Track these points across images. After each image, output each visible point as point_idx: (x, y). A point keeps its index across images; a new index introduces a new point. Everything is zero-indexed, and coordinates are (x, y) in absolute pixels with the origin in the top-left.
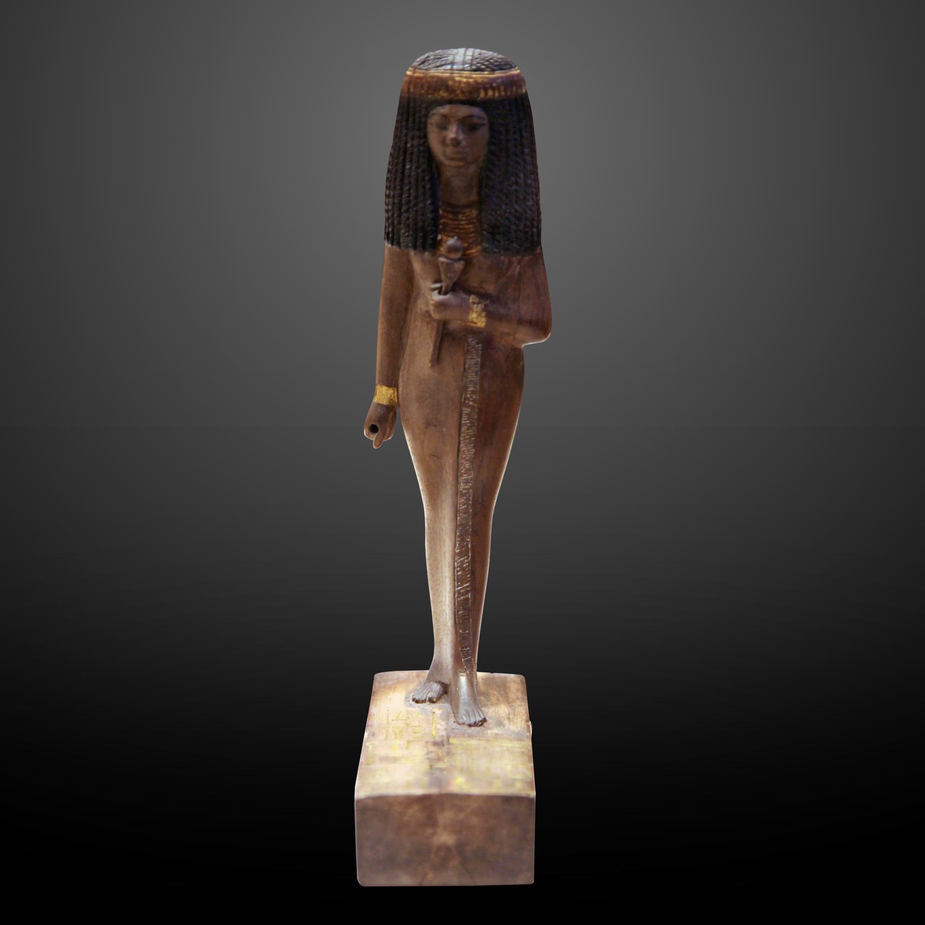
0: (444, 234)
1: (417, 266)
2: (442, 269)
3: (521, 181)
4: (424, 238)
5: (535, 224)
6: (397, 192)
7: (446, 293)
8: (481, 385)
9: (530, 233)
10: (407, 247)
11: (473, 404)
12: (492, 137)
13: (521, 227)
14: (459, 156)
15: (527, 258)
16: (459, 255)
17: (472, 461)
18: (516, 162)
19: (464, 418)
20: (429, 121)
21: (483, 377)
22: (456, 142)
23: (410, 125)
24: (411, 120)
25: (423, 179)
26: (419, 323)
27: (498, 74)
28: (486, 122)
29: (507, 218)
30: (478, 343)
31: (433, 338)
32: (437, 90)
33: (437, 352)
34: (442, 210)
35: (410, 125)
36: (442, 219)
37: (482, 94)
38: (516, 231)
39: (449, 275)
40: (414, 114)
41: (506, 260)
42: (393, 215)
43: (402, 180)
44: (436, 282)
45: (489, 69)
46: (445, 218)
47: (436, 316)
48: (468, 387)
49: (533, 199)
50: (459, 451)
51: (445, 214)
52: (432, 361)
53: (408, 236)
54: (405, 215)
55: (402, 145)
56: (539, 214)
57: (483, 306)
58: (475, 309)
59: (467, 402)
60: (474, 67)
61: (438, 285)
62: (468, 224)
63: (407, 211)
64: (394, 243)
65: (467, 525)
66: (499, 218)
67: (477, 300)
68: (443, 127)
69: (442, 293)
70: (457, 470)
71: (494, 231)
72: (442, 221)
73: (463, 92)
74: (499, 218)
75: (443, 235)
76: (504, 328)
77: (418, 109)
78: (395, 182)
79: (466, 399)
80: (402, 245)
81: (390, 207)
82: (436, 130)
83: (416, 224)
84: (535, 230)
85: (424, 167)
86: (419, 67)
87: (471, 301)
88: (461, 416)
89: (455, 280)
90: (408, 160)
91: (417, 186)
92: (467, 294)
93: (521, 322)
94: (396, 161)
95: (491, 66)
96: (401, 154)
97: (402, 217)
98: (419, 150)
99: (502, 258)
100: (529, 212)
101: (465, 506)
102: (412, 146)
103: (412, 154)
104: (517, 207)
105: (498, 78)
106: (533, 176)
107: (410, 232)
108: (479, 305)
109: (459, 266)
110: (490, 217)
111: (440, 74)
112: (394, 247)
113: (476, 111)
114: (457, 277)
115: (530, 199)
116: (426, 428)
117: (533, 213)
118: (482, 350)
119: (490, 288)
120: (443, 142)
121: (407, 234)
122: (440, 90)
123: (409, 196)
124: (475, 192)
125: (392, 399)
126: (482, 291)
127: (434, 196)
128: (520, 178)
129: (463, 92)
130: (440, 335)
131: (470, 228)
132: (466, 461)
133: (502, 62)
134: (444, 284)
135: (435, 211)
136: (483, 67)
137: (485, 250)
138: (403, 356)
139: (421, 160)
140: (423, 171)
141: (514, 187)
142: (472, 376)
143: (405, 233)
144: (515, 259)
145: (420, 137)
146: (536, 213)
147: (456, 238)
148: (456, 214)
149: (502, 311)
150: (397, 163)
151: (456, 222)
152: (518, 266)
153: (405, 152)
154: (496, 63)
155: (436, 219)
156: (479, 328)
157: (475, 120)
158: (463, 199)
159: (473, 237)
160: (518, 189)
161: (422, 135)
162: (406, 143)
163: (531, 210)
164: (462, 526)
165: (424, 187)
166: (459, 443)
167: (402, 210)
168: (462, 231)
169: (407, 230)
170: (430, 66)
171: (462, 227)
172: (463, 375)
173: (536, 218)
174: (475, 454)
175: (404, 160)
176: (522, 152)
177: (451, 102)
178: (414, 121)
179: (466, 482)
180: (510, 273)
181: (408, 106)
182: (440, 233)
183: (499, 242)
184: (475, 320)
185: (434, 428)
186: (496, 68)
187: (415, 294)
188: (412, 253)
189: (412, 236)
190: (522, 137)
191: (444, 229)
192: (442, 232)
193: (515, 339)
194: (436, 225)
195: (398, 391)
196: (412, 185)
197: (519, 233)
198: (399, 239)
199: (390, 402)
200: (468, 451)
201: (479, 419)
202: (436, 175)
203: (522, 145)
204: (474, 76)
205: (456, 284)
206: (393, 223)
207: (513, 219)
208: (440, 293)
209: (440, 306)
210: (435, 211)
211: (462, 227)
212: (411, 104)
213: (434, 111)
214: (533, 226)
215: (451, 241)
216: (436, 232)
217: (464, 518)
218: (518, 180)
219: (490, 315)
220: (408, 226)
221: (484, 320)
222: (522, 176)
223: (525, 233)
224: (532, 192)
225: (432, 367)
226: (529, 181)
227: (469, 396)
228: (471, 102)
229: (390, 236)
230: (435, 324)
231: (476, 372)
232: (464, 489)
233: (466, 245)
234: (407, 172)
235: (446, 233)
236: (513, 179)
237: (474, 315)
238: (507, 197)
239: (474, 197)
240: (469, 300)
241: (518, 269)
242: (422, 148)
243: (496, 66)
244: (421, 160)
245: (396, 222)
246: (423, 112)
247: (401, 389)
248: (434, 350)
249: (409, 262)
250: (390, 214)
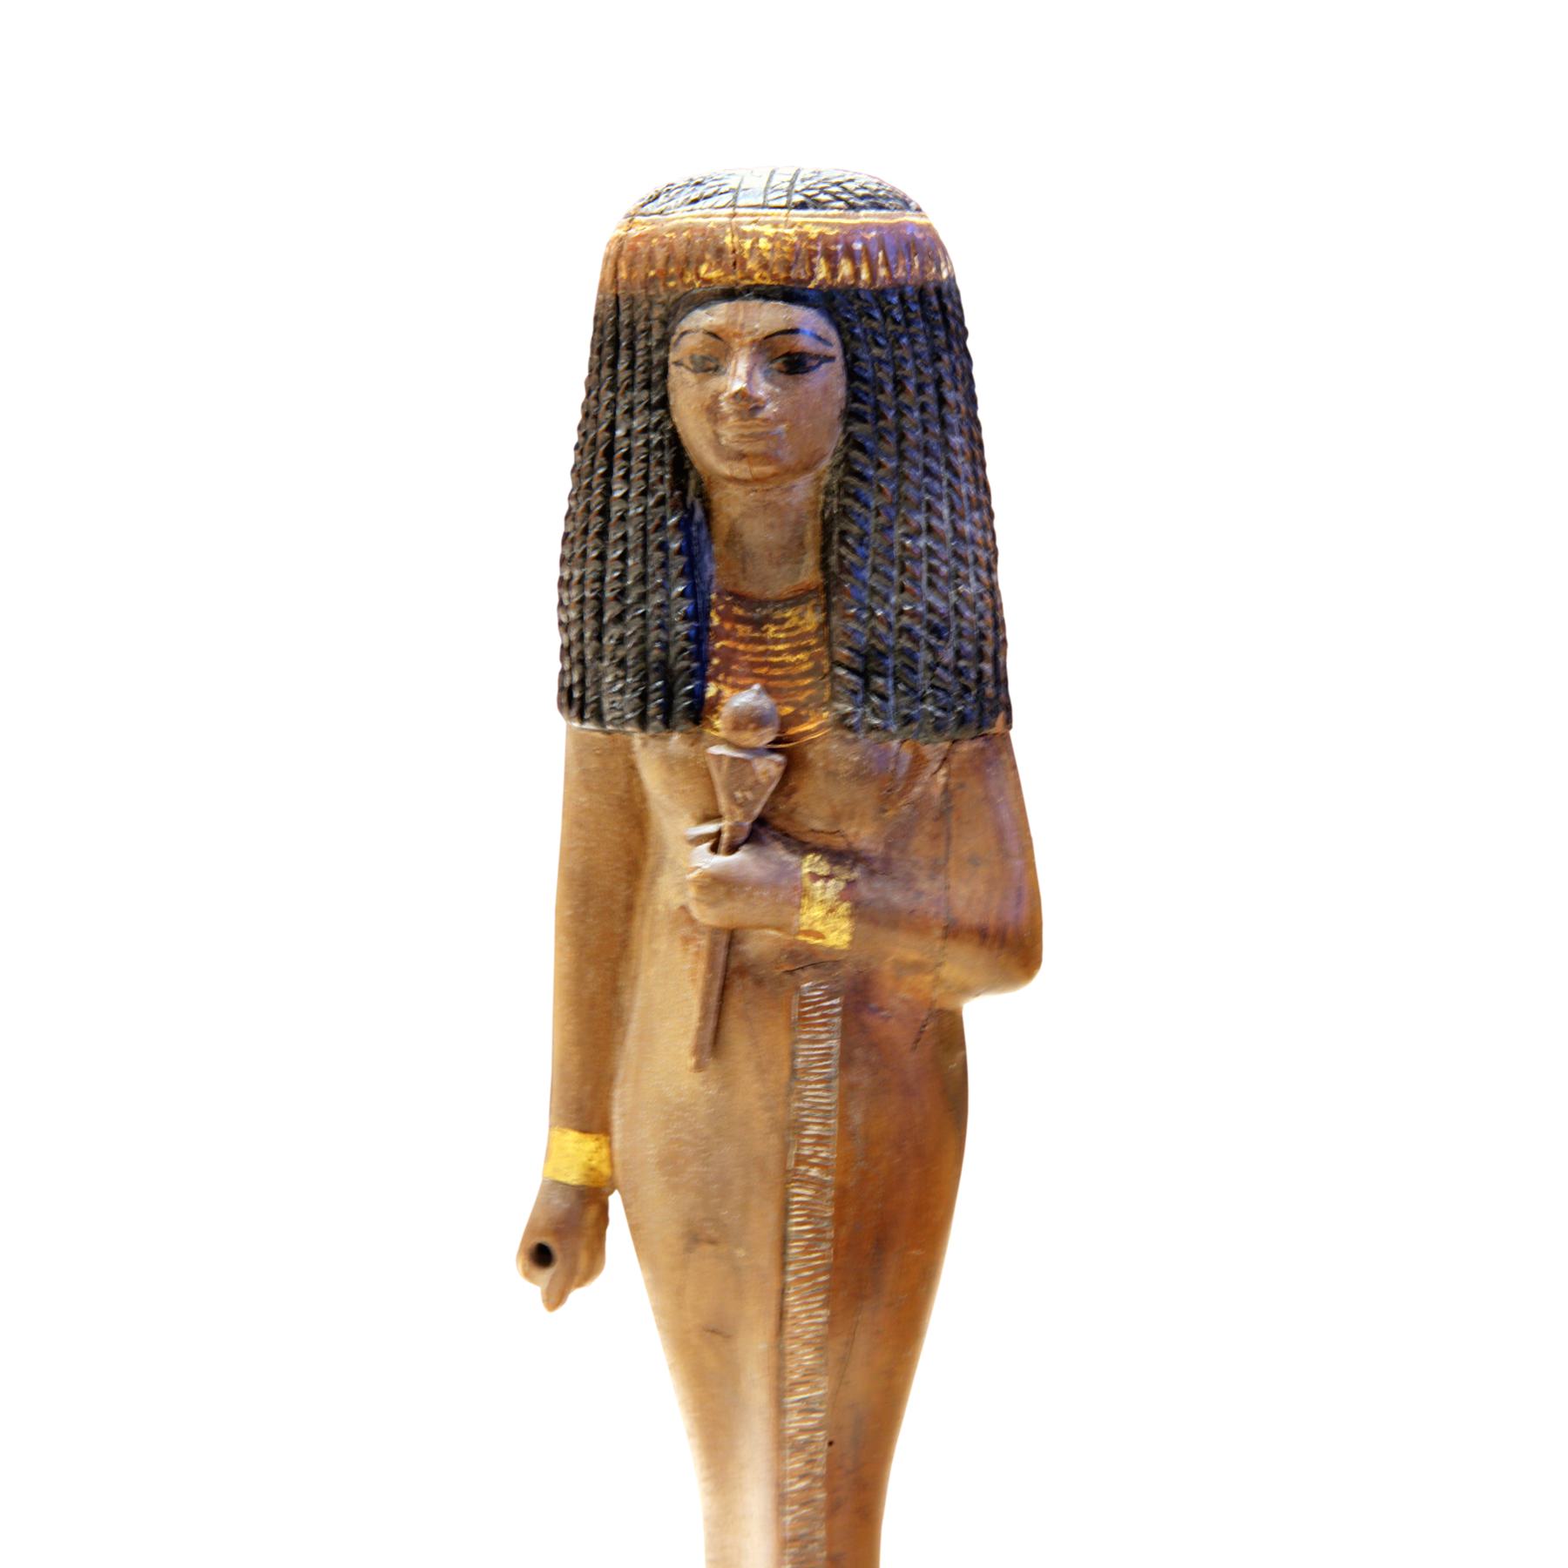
0: (725, 682)
1: (652, 777)
2: (718, 778)
3: (944, 527)
4: (669, 693)
5: (989, 649)
6: (591, 569)
7: (732, 849)
8: (844, 1119)
9: (973, 675)
10: (622, 721)
11: (820, 1176)
12: (853, 396)
13: (948, 656)
14: (760, 447)
15: (965, 748)
16: (768, 736)
17: (821, 1348)
18: (928, 471)
19: (797, 1215)
20: (673, 357)
21: (847, 1094)
22: (747, 404)
23: (623, 375)
24: (623, 364)
25: (661, 527)
26: (662, 945)
27: (868, 217)
28: (835, 350)
29: (906, 631)
30: (831, 995)
31: (700, 984)
32: (690, 262)
33: (711, 1024)
34: (719, 613)
35: (623, 375)
36: (719, 639)
37: (822, 272)
38: (931, 668)
39: (738, 794)
40: (631, 347)
41: (907, 753)
42: (581, 637)
43: (603, 534)
44: (707, 819)
45: (841, 204)
46: (727, 636)
47: (706, 916)
48: (804, 1126)
49: (978, 579)
50: (782, 1314)
51: (727, 626)
52: (698, 1050)
53: (622, 692)
54: (614, 631)
55: (603, 435)
56: (999, 625)
57: (842, 885)
58: (818, 895)
59: (803, 1168)
60: (797, 198)
61: (711, 828)
62: (794, 651)
63: (619, 619)
64: (587, 716)
65: (813, 1541)
66: (882, 629)
67: (824, 869)
68: (709, 365)
69: (722, 847)
70: (780, 1372)
71: (868, 664)
72: (718, 645)
73: (765, 266)
74: (882, 629)
75: (722, 687)
76: (904, 948)
77: (641, 326)
78: (584, 542)
79: (801, 1160)
80: (608, 718)
81: (573, 614)
82: (690, 377)
83: (643, 655)
84: (987, 667)
85: (662, 490)
86: (643, 210)
87: (806, 870)
88: (785, 1213)
89: (757, 811)
90: (618, 473)
91: (645, 546)
92: (794, 852)
93: (952, 931)
94: (585, 482)
95: (844, 196)
96: (600, 460)
97: (605, 640)
98: (647, 444)
99: (895, 743)
100: (968, 614)
101: (803, 1484)
102: (628, 434)
103: (627, 456)
104: (932, 598)
105: (867, 227)
106: (976, 516)
107: (629, 680)
108: (832, 882)
109: (769, 767)
110: (853, 625)
111: (701, 220)
112: (589, 726)
113: (806, 318)
114: (764, 799)
115: (972, 579)
116: (688, 1250)
117: (981, 617)
118: (843, 1014)
119: (863, 835)
120: (712, 411)
121: (619, 686)
122: (701, 261)
123: (622, 577)
124: (811, 559)
125: (592, 1169)
126: (839, 843)
127: (691, 571)
128: (940, 517)
129: (765, 266)
130: (720, 971)
131: (801, 662)
132: (807, 1344)
133: (878, 190)
134: (725, 824)
135: (699, 615)
136: (822, 197)
137: (842, 721)
138: (622, 1043)
139: (656, 472)
140: (661, 502)
141: (922, 542)
142: (817, 1094)
143: (613, 683)
144: (933, 750)
145: (649, 407)
146: (988, 616)
147: (756, 687)
148: (758, 624)
149: (897, 898)
150: (589, 486)
151: (761, 648)
152: (943, 771)
153: (609, 453)
154: (861, 192)
155: (700, 636)
156: (831, 950)
157: (804, 343)
158: (780, 585)
159: (807, 687)
160: (935, 547)
161: (655, 399)
162: (612, 428)
163: (973, 607)
164: (798, 1544)
165: (663, 547)
166: (783, 1293)
167: (606, 619)
168: (778, 672)
169: (620, 673)
170: (672, 203)
171: (775, 660)
172: (790, 1091)
173: (990, 633)
174: (830, 1323)
175: (608, 474)
176: (946, 445)
177: (730, 294)
178: (631, 366)
179: (807, 1409)
180: (917, 790)
181: (616, 322)
182: (714, 678)
183: (883, 697)
184: (819, 927)
185: (709, 1249)
186: (862, 203)
187: (650, 863)
188: (637, 738)
189: (634, 690)
190: (942, 401)
191: (725, 669)
192: (721, 677)
193: (938, 981)
194: (702, 656)
195: (610, 1144)
196: (631, 546)
197: (939, 671)
198: (598, 701)
199: (586, 1175)
200: (807, 1315)
201: (838, 1220)
202: (699, 514)
203: (943, 424)
204: (799, 220)
205: (761, 822)
206: (582, 661)
207: (924, 633)
208: (714, 849)
209: (717, 886)
210: (699, 615)
211: (775, 660)
212: (624, 318)
213: (686, 324)
214: (981, 655)
215: (746, 698)
216: (702, 676)
217: (801, 1519)
218: (935, 522)
219: (862, 912)
220: (622, 664)
221: (846, 925)
222: (946, 512)
223: (959, 672)
224: (976, 560)
225: (699, 1067)
226: (967, 528)
227: (806, 1151)
228: (790, 294)
229: (576, 694)
230: (704, 942)
231: (827, 1081)
232: (803, 1431)
233: (788, 710)
234: (616, 510)
235: (730, 680)
236: (920, 519)
237: (817, 912)
238: (903, 570)
239: (809, 574)
240: (799, 867)
241: (941, 779)
242: (655, 438)
243: (863, 197)
244: (656, 472)
245: (589, 657)
246: (656, 334)
247: (617, 1136)
248: (704, 1018)
249: (632, 769)
250: (574, 632)
